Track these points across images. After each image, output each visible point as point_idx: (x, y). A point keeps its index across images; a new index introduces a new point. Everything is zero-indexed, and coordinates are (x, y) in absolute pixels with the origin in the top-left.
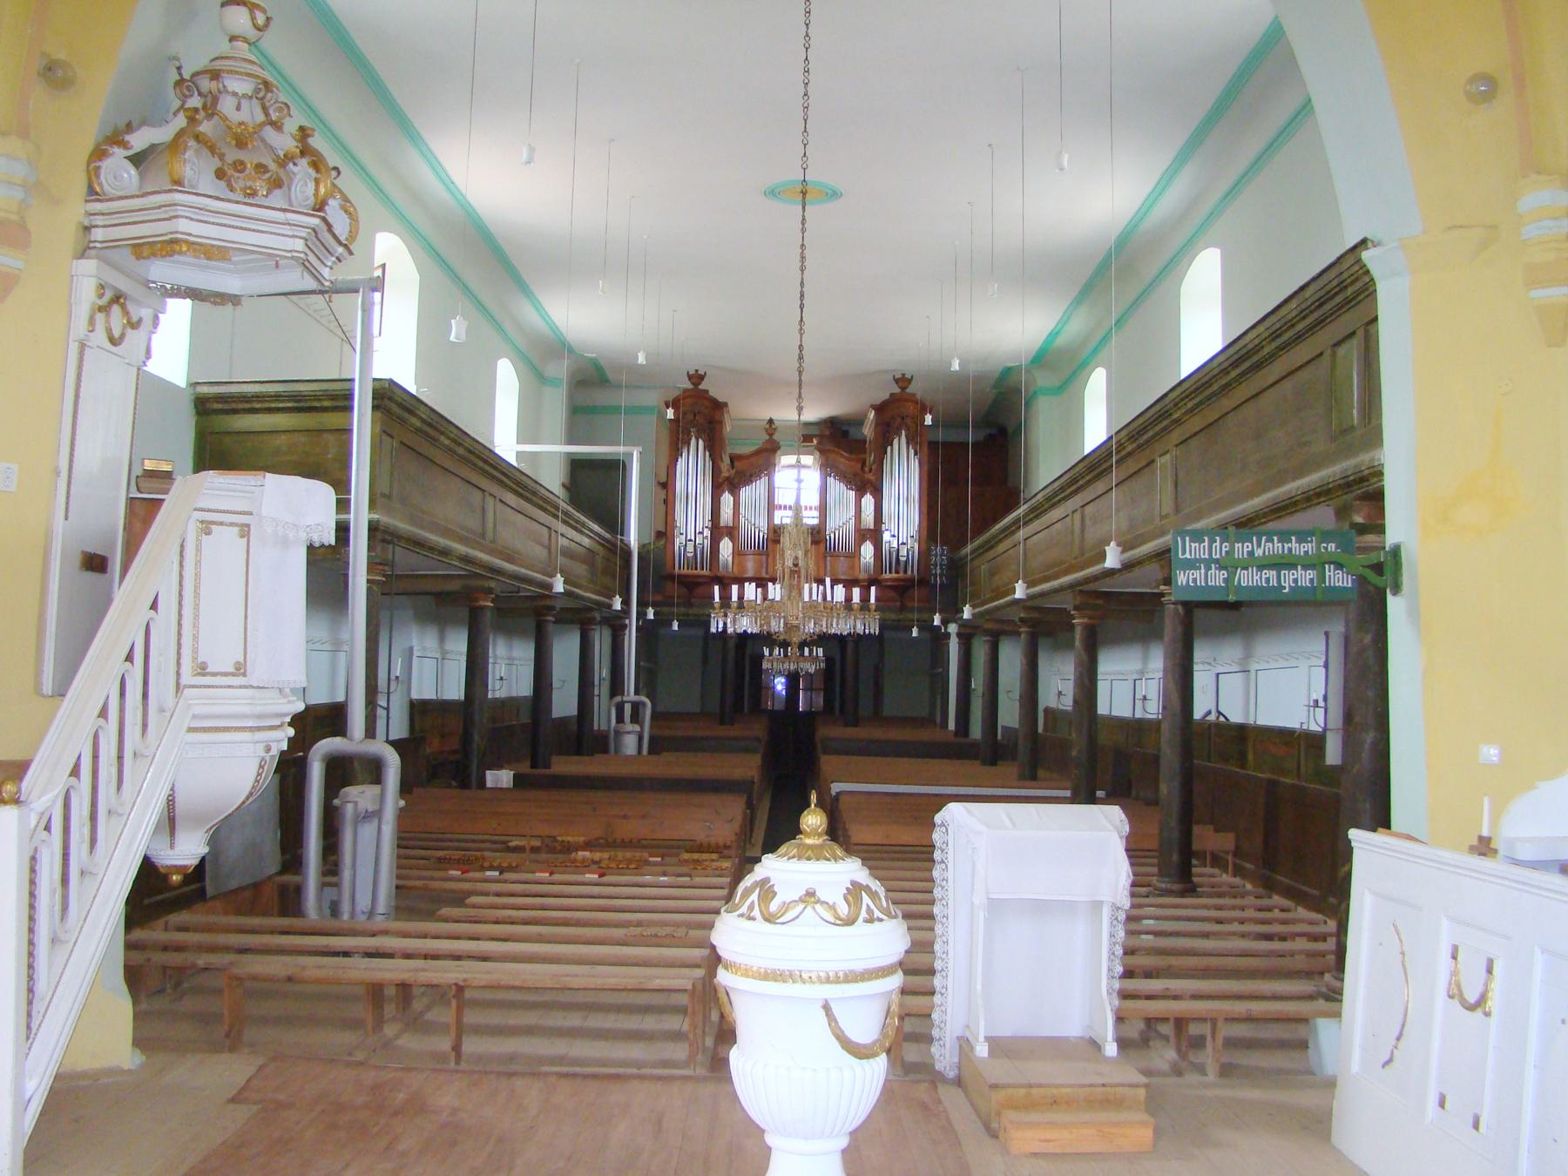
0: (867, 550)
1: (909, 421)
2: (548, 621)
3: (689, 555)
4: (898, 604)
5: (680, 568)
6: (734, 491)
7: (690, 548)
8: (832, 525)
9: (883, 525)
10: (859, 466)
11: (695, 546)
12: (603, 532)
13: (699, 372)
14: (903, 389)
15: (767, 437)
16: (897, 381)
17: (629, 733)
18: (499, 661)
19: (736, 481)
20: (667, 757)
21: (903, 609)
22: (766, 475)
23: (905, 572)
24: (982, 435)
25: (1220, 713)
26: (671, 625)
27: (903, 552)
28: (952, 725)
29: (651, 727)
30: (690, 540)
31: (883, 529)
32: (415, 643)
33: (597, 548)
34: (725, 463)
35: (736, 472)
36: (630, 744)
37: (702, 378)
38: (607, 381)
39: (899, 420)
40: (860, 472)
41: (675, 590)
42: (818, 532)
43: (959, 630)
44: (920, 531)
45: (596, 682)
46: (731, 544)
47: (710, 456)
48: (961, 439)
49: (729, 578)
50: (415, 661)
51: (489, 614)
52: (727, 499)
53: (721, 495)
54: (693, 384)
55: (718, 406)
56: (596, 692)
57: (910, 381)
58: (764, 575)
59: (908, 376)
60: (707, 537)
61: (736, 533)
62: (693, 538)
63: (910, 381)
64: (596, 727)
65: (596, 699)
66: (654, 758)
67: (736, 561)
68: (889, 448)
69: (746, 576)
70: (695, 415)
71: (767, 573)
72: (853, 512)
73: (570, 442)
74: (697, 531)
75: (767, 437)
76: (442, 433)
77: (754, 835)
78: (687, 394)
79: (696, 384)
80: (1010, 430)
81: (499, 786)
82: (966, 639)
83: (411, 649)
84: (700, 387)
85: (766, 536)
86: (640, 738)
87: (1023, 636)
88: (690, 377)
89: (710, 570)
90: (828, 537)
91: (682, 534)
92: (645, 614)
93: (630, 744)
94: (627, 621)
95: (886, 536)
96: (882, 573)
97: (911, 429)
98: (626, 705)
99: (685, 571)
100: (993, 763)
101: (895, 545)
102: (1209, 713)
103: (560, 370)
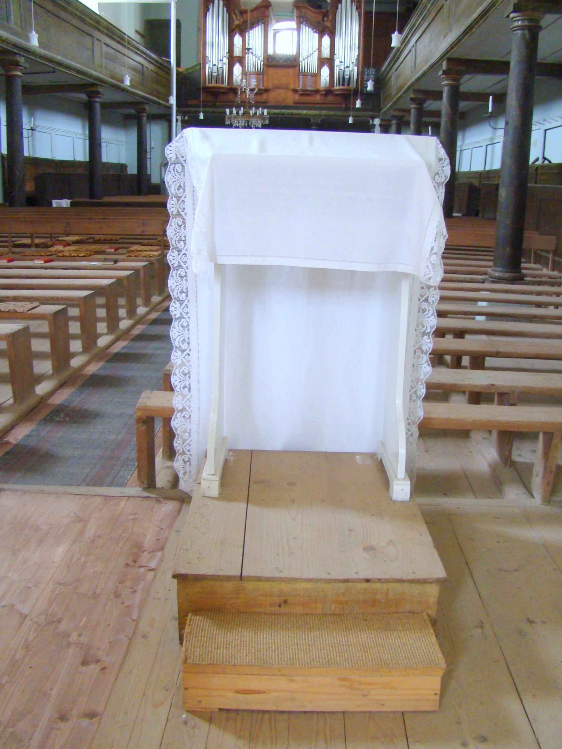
0: (325, 72)
2: (96, 101)
4: (344, 106)
5: (209, 83)
6: (242, 35)
8: (304, 56)
9: (335, 56)
10: (321, 17)
11: (218, 69)
22: (262, 23)
23: (349, 85)
25: (545, 159)
26: (199, 116)
27: (347, 72)
31: (335, 58)
33: (146, 64)
40: (321, 22)
42: (295, 60)
43: (381, 122)
45: (148, 150)
46: (240, 68)
47: (227, 11)
52: (238, 39)
58: (261, 87)
62: (217, 64)
65: (148, 161)
68: (340, 6)
71: (263, 86)
72: (316, 46)
74: (219, 59)
85: (262, 63)
87: (412, 111)
89: (228, 84)
90: (301, 64)
91: (209, 61)
95: (337, 62)
101: (342, 68)
102: (537, 160)
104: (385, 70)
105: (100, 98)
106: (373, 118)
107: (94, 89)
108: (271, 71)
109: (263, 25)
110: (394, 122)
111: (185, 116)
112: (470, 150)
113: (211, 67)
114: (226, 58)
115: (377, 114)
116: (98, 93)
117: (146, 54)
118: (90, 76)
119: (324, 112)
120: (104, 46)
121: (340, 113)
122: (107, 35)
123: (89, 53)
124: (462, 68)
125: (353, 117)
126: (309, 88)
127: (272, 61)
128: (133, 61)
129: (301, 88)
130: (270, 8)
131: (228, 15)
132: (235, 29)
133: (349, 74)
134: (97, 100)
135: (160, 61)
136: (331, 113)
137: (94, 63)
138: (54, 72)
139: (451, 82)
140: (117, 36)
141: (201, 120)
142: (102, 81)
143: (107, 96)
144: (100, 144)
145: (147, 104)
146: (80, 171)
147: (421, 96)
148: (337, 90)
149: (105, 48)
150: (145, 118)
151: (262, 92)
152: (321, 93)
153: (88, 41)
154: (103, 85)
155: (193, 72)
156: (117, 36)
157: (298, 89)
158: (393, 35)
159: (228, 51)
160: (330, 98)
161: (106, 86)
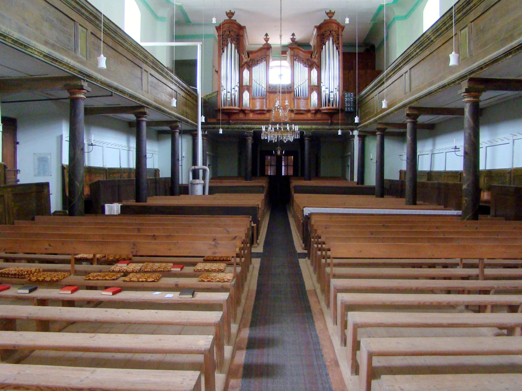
0: (314, 96)
1: (333, 33)
2: (143, 121)
4: (329, 121)
5: (224, 106)
7: (229, 95)
9: (322, 84)
10: (310, 55)
12: (181, 82)
13: (231, 11)
14: (330, 17)
15: (265, 42)
16: (327, 14)
17: (197, 184)
19: (250, 64)
20: (217, 195)
21: (332, 124)
23: (333, 106)
24: (362, 50)
27: (332, 96)
28: (356, 179)
29: (210, 182)
30: (229, 92)
35: (250, 60)
36: (199, 190)
37: (233, 14)
38: (190, 22)
39: (329, 32)
40: (310, 58)
41: (220, 116)
42: (291, 87)
44: (339, 86)
45: (180, 159)
46: (248, 94)
48: (354, 51)
49: (248, 110)
53: (243, 70)
55: (242, 28)
56: (180, 164)
57: (333, 13)
58: (265, 108)
59: (333, 11)
61: (251, 88)
62: (230, 91)
63: (333, 13)
64: (180, 183)
65: (180, 167)
66: (211, 196)
67: (251, 102)
68: (324, 47)
70: (230, 32)
71: (266, 108)
74: (232, 88)
75: (265, 42)
77: (259, 238)
78: (226, 22)
79: (230, 17)
80: (376, 46)
81: (112, 214)
82: (362, 138)
83: (61, 136)
84: (232, 19)
86: (204, 188)
87: (408, 124)
88: (227, 14)
89: (239, 107)
90: (295, 90)
91: (224, 89)
93: (199, 190)
95: (323, 89)
96: (322, 107)
97: (335, 37)
98: (200, 170)
99: (227, 107)
100: (382, 196)
101: (328, 92)
104: (366, 93)
105: (146, 117)
106: (352, 130)
107: (142, 110)
109: (265, 62)
110: (378, 133)
111: (205, 131)
112: (444, 154)
114: (237, 87)
115: (356, 127)
116: (145, 113)
117: (179, 83)
118: (139, 100)
119: (314, 127)
120: (149, 75)
121: (327, 127)
122: (153, 68)
123: (139, 80)
124: (482, 87)
125: (341, 130)
126: (302, 109)
127: (273, 89)
128: (169, 88)
129: (295, 108)
130: (271, 49)
131: (238, 55)
132: (244, 65)
133: (333, 97)
134: (144, 119)
135: (189, 89)
136: (320, 127)
137: (142, 90)
139: (472, 99)
140: (160, 68)
141: (221, 134)
142: (148, 104)
143: (152, 116)
144: (146, 156)
145: (179, 122)
146: (125, 177)
147: (415, 112)
148: (324, 110)
149: (151, 79)
150: (178, 133)
151: (264, 112)
152: (311, 112)
153: (138, 72)
154: (149, 107)
155: (211, 97)
156: (160, 68)
157: (294, 109)
158: (450, 55)
160: (319, 116)
161: (151, 108)
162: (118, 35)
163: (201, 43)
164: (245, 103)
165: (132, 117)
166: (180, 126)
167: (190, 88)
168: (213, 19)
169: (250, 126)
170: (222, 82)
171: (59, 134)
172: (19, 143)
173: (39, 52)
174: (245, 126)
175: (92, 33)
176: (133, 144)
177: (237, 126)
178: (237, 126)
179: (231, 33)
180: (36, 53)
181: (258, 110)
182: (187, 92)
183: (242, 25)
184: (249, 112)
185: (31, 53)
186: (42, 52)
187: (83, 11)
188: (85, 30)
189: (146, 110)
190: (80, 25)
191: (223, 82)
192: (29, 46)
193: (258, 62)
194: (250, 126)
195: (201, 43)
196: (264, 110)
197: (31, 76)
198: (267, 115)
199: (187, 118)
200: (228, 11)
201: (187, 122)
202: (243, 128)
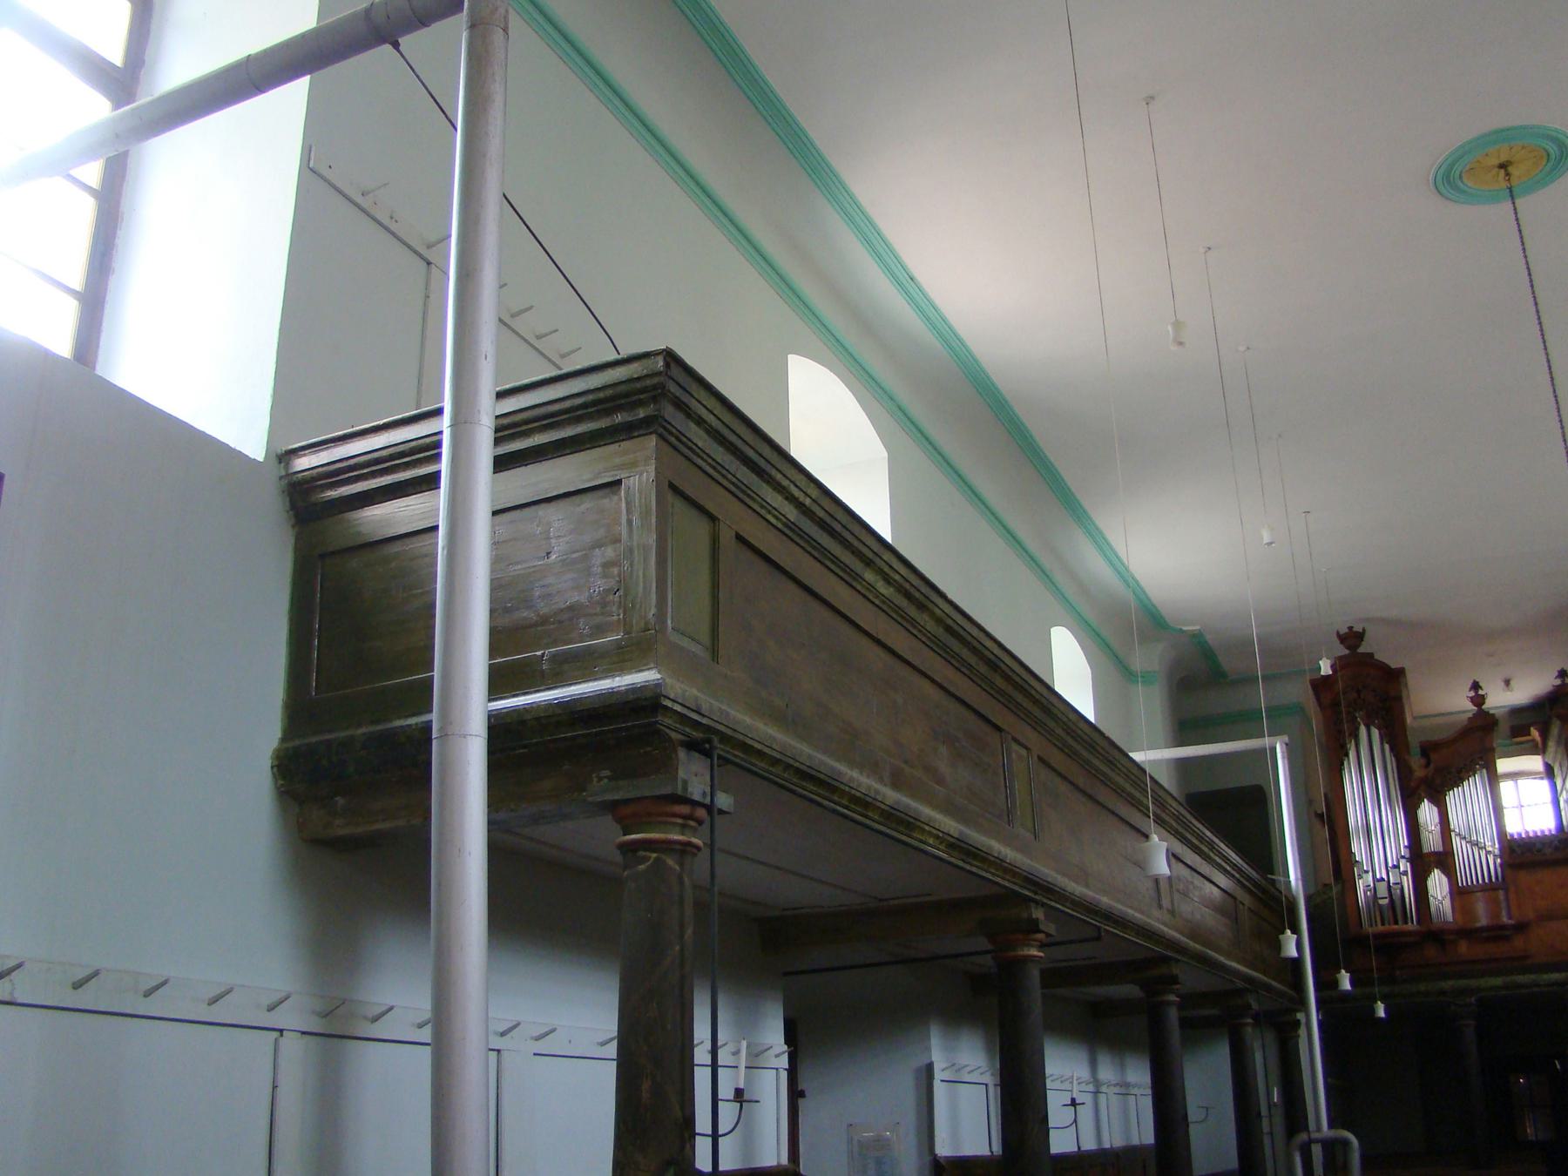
2: (1169, 1003)
3: (1382, 902)
7: (1382, 890)
11: (1389, 886)
13: (1354, 629)
18: (1104, 1089)
22: (1482, 767)
32: (938, 1058)
33: (1241, 894)
34: (1416, 761)
45: (1264, 1112)
46: (1445, 879)
47: (1392, 750)
50: (940, 1090)
51: (1035, 973)
52: (1427, 813)
54: (1348, 648)
55: (1394, 676)
58: (1505, 920)
60: (1405, 873)
62: (1384, 876)
65: (1267, 1141)
69: (1478, 925)
70: (1359, 692)
71: (1510, 918)
73: (1181, 743)
74: (1390, 865)
76: (869, 563)
83: (929, 1068)
84: (1361, 650)
88: (1342, 639)
91: (1367, 872)
92: (1335, 984)
94: (1300, 1016)
99: (1380, 928)
103: (1150, 659)
108: (1524, 877)
109: (1484, 771)
113: (1372, 885)
137: (1160, 907)
138: (1098, 938)
140: (1194, 833)
141: (1381, 1019)
151: (1507, 933)
156: (1194, 833)
159: (1406, 844)
162: (1099, 753)
163: (1286, 738)
164: (1438, 909)
165: (1128, 990)
166: (1255, 1006)
167: (1266, 879)
168: (1320, 662)
169: (1463, 983)
170: (1355, 848)
171: (922, 1061)
172: (806, 1093)
173: (937, 837)
174: (1447, 985)
175: (1040, 758)
176: (1139, 1075)
177: (1422, 987)
178: (1422, 987)
179: (1362, 697)
180: (931, 841)
181: (1482, 929)
182: (1260, 895)
183: (1393, 666)
184: (1451, 937)
185: (921, 841)
186: (946, 837)
187: (1020, 698)
188: (1024, 752)
189: (1175, 971)
190: (1015, 740)
191: (1358, 848)
192: (919, 823)
193: (1462, 775)
194: (1463, 983)
195: (1286, 738)
196: (1503, 927)
197: (880, 900)
198: (1518, 942)
199: (1265, 975)
200: (1344, 630)
201: (1268, 988)
202: (1443, 993)
